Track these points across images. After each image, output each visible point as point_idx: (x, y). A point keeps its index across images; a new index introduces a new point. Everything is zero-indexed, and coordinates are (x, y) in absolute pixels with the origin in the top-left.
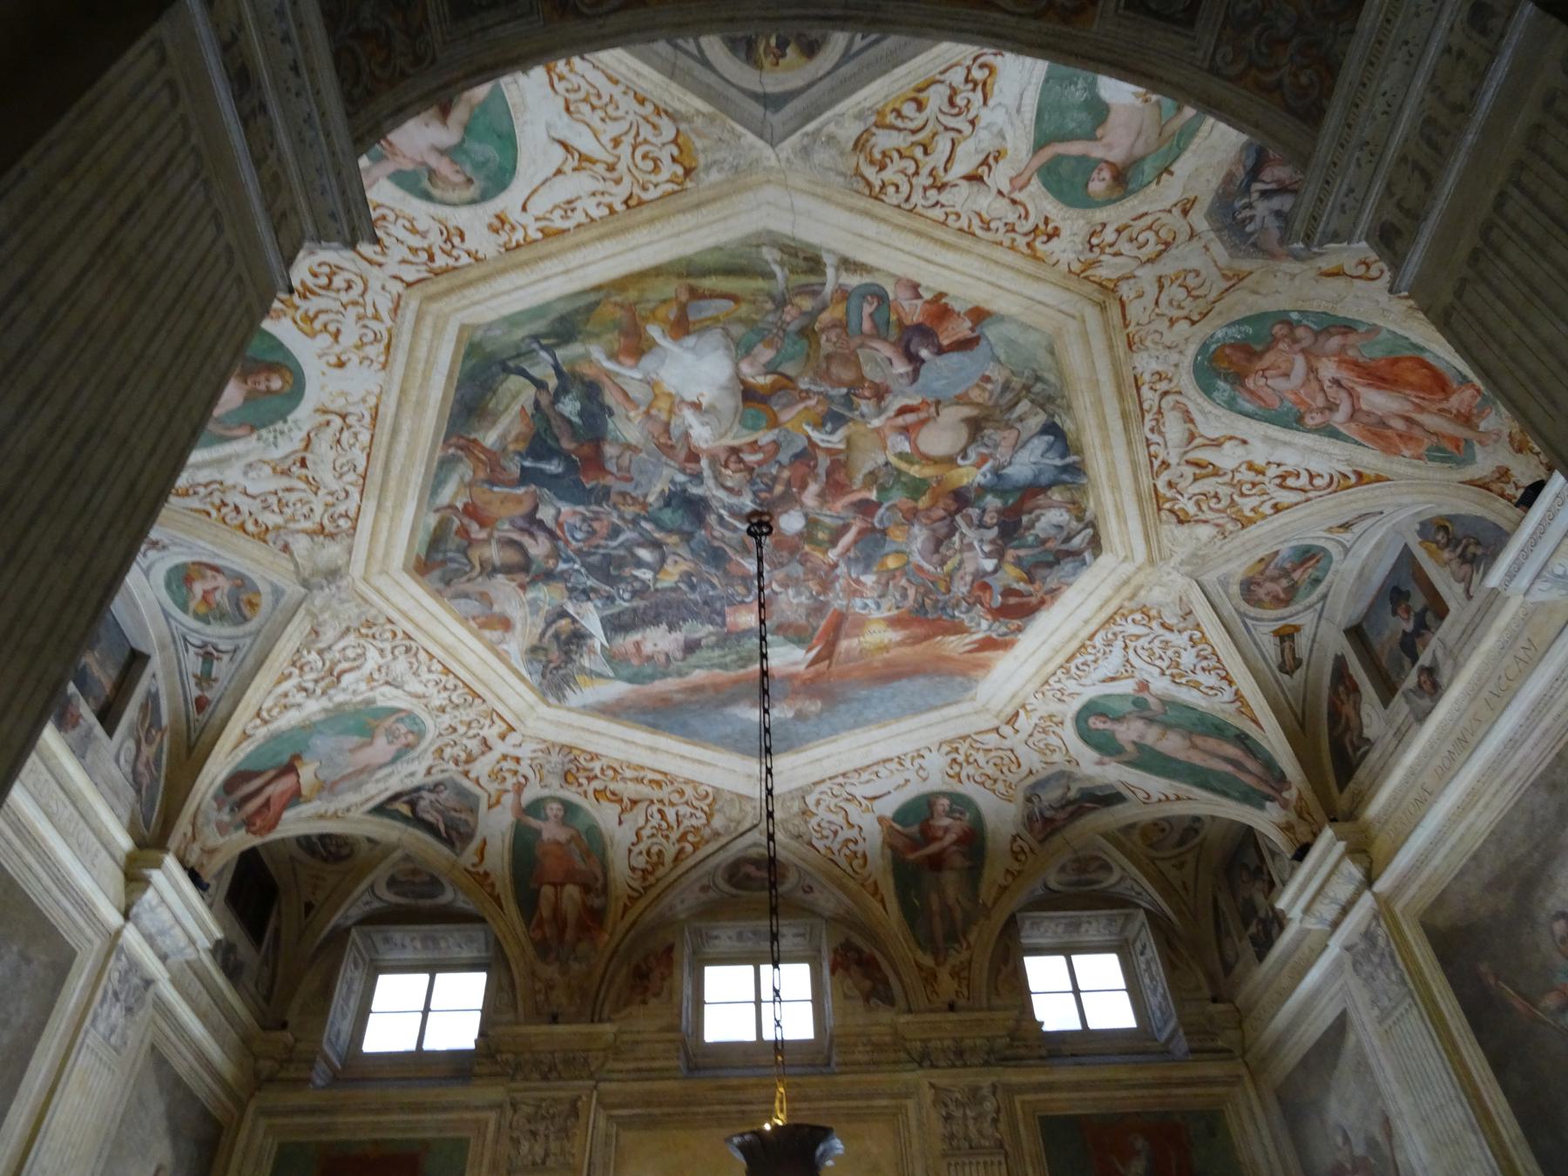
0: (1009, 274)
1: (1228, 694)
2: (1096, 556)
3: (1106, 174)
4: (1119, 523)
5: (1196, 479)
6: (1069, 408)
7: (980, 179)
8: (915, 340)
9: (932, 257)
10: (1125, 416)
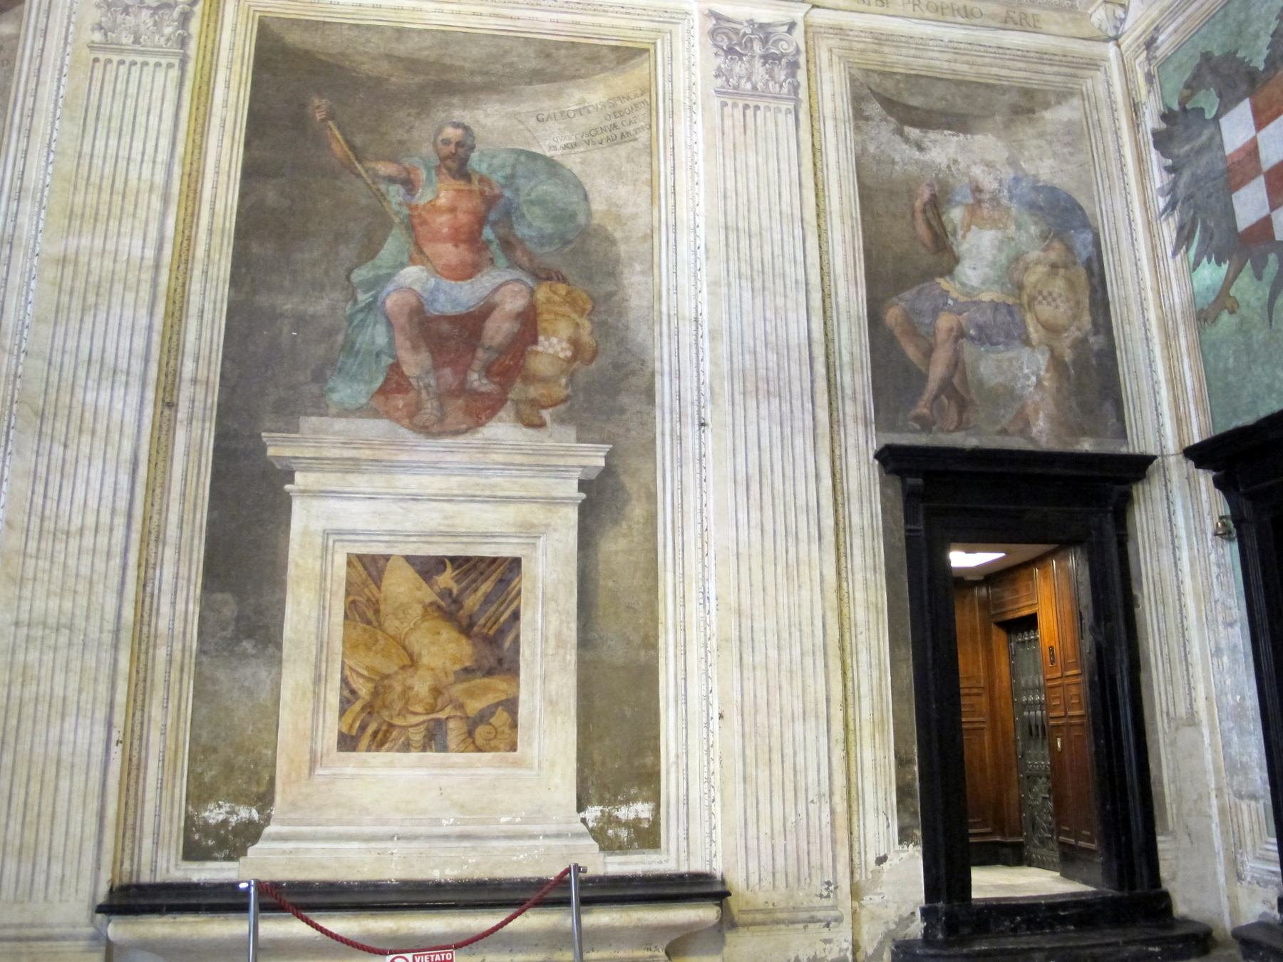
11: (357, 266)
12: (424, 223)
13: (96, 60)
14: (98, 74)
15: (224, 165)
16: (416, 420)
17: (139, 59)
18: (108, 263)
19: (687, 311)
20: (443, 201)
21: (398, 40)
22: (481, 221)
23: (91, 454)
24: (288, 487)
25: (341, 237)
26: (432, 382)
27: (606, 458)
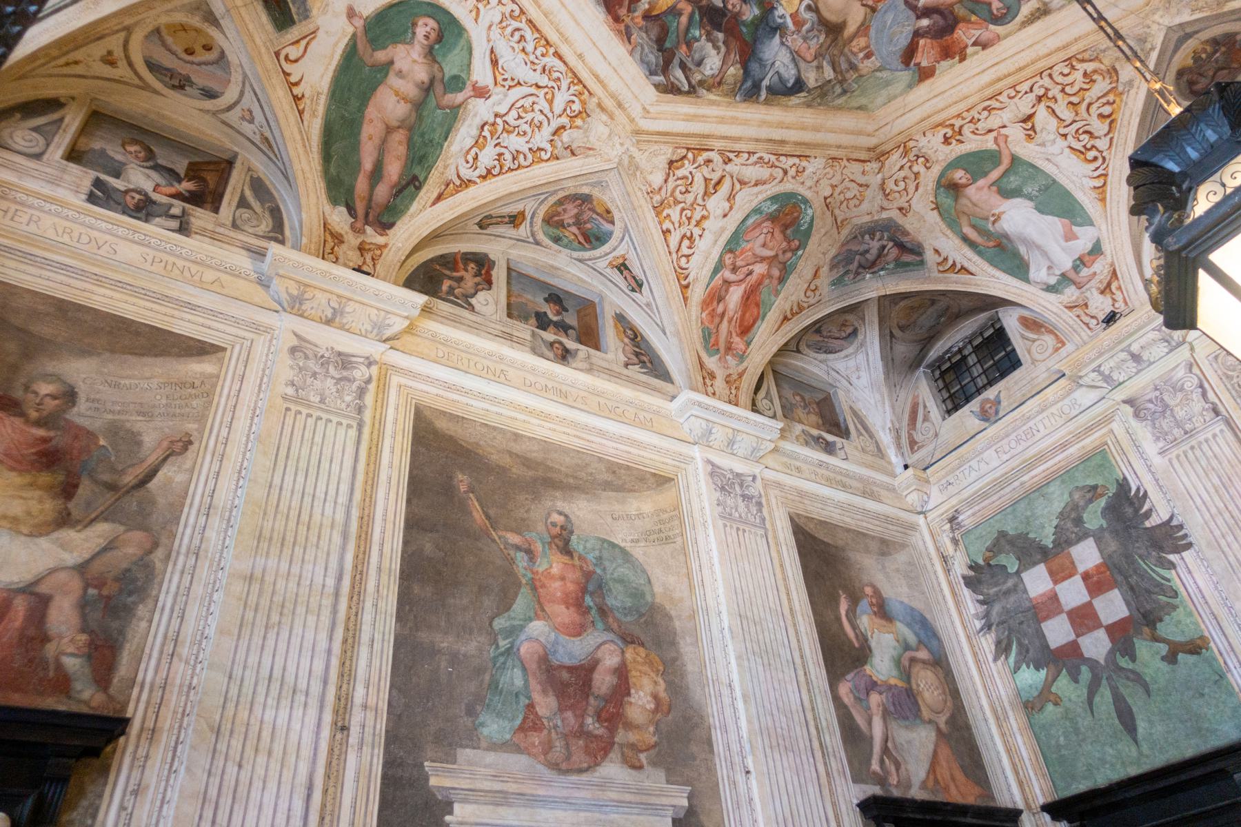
0: (941, 105)
1: (466, 173)
2: (657, 86)
3: (964, 181)
4: (685, 115)
5: (706, 179)
6: (809, 105)
7: (1024, 121)
8: (941, 22)
9: (996, 68)
10: (782, 142)
11: (497, 615)
12: (543, 586)
13: (288, 409)
14: (289, 421)
15: (390, 516)
16: (549, 756)
17: (325, 416)
18: (292, 586)
19: (725, 680)
20: (556, 570)
21: (515, 440)
22: (584, 590)
23: (266, 776)
24: (448, 818)
25: (483, 590)
26: (559, 723)
27: (689, 798)
